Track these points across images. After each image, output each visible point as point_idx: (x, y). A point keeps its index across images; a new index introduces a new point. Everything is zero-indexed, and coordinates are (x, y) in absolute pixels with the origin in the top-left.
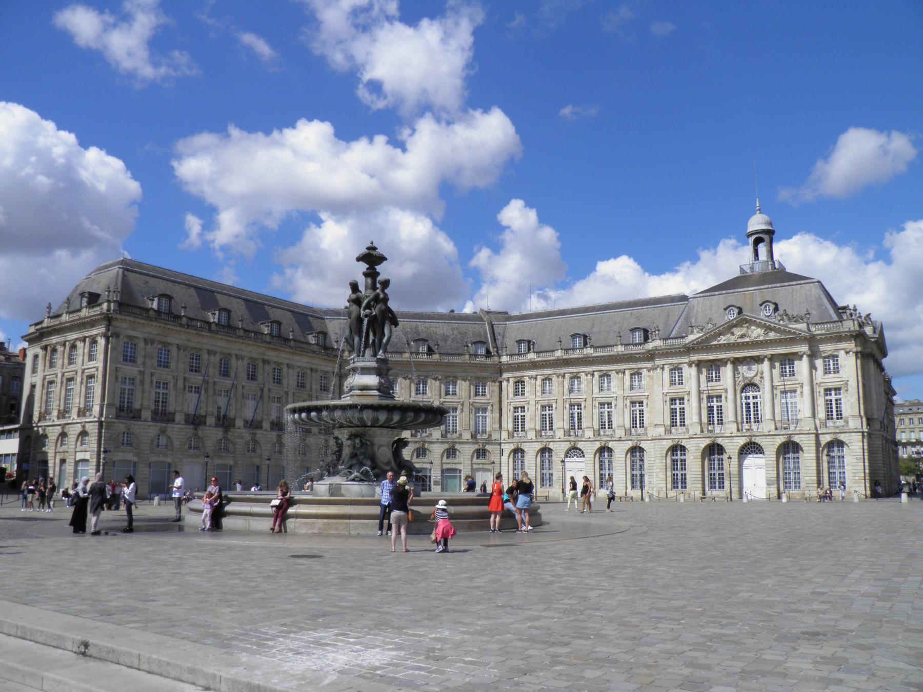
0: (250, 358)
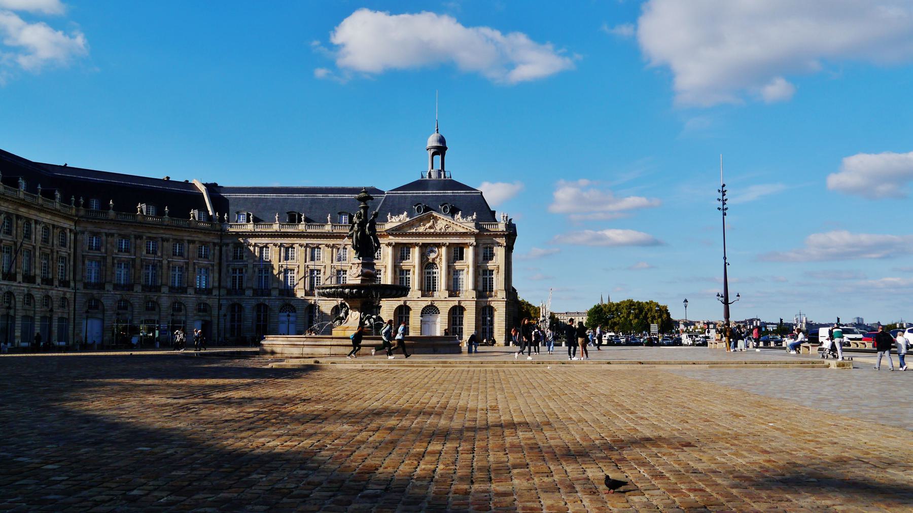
0: (6, 213)
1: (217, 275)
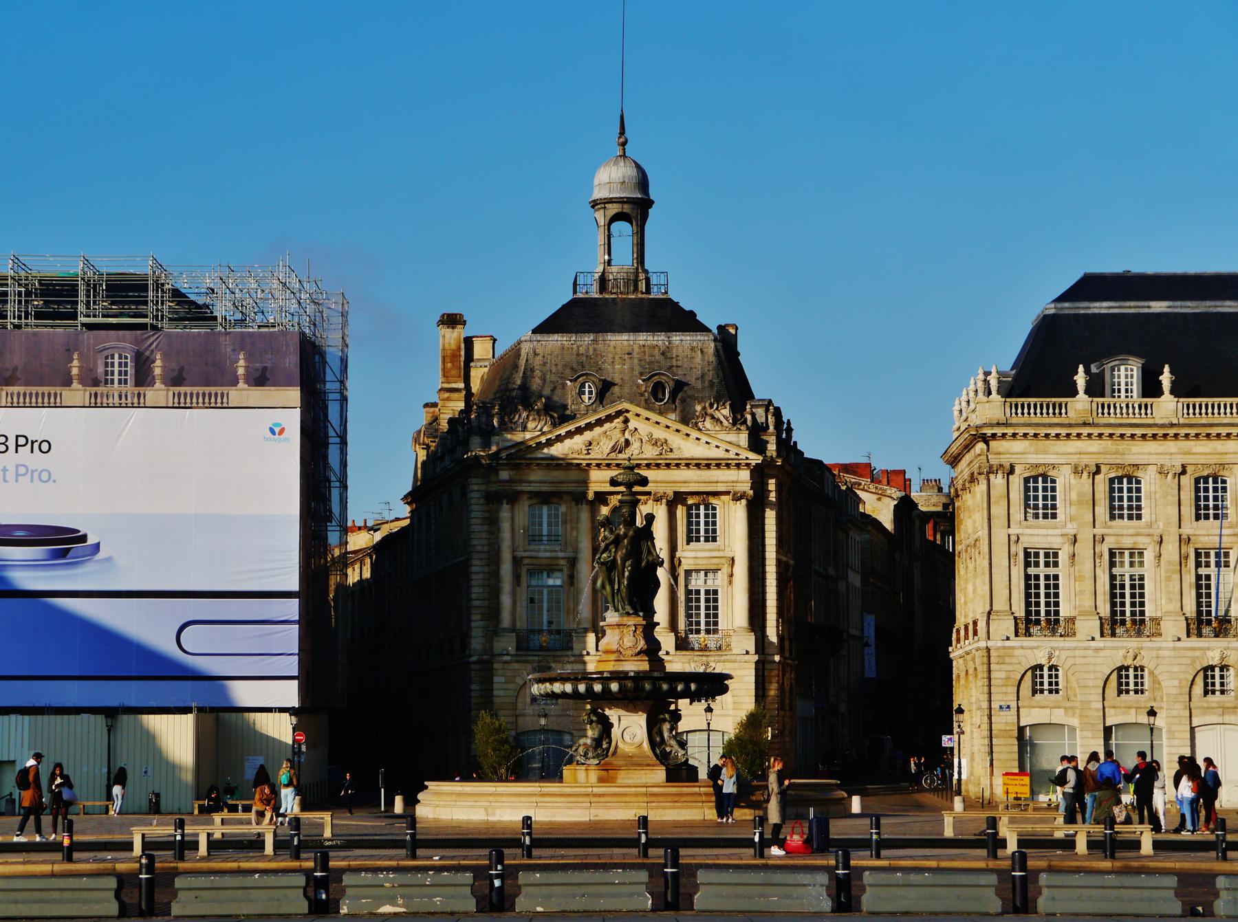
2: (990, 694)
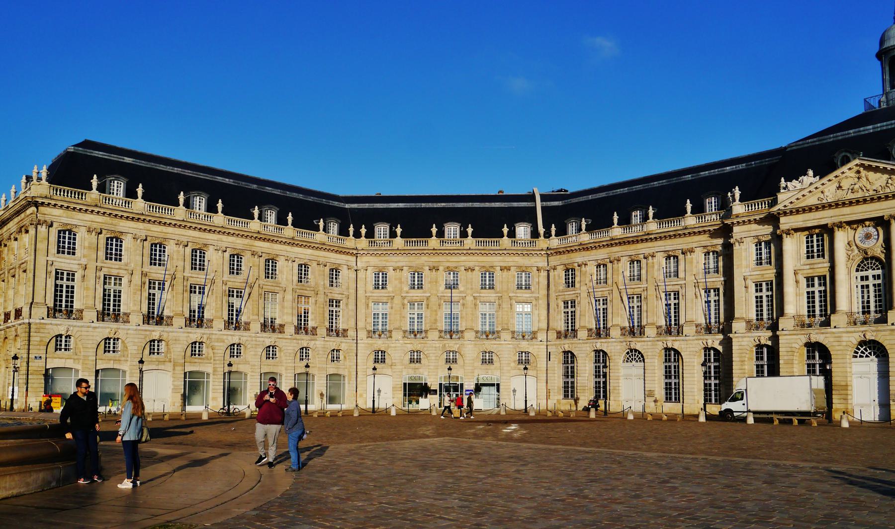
1: (544, 313)
2: (29, 349)
